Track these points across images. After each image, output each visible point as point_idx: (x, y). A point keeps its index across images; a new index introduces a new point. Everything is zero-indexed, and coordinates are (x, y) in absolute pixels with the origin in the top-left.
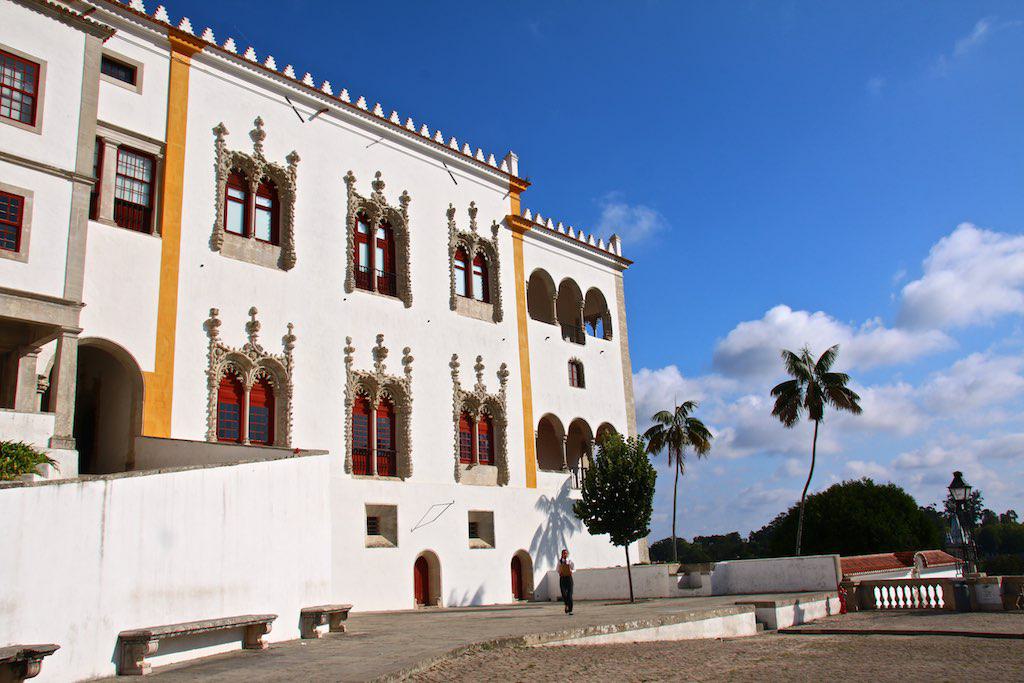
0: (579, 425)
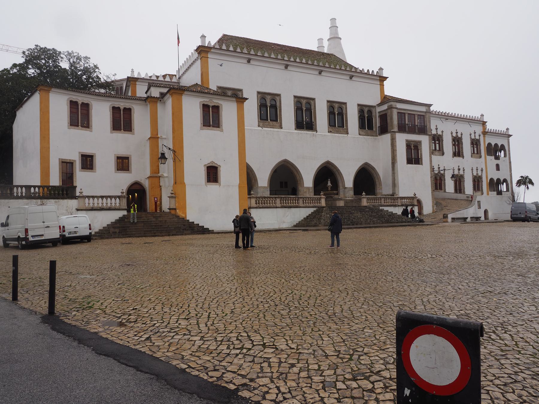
0: (498, 180)
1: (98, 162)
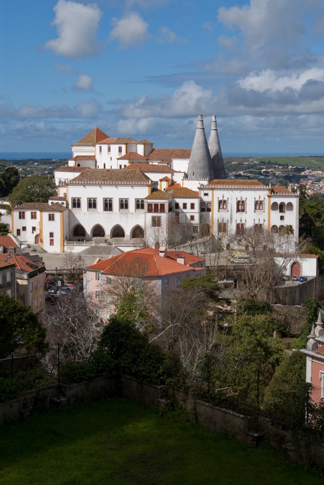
1: (27, 229)
